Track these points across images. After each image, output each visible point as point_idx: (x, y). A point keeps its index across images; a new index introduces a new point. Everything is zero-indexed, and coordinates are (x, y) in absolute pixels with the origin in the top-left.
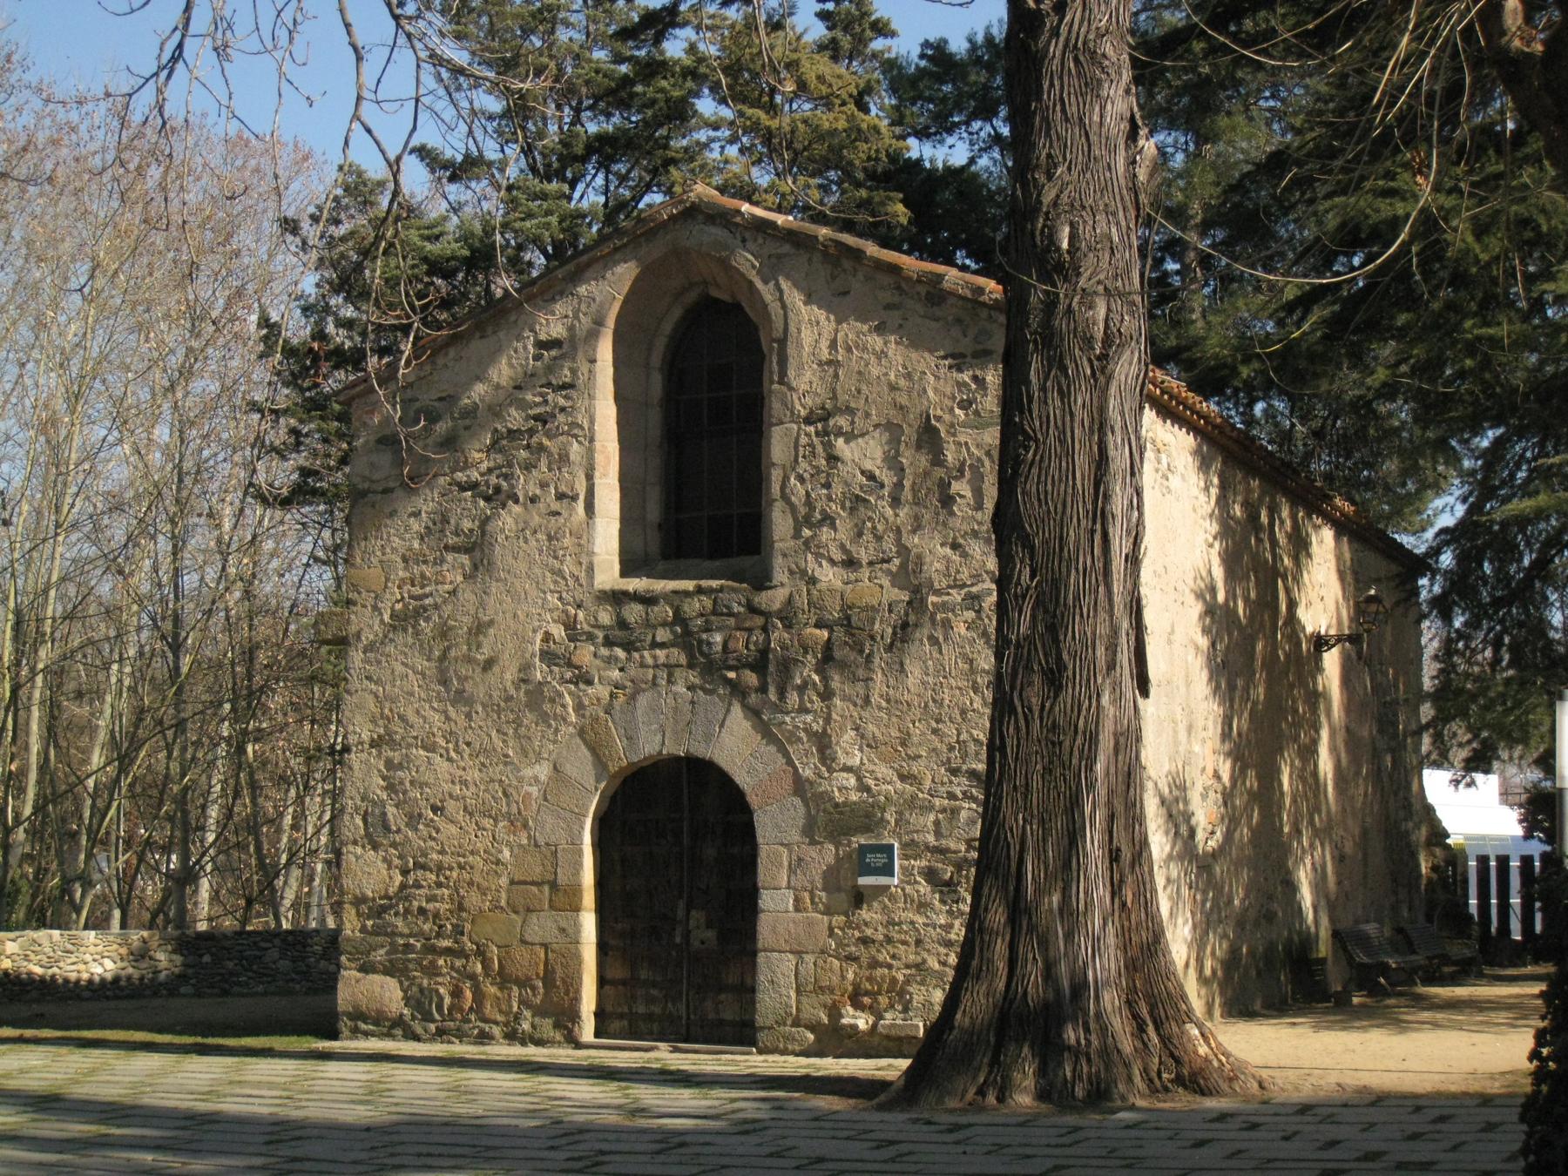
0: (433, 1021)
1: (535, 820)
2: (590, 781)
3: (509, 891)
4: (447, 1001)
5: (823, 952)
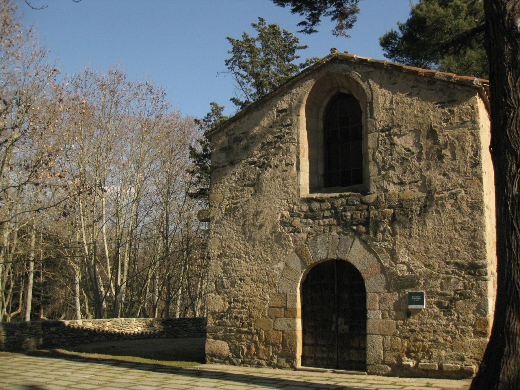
0: (240, 358)
1: (279, 284)
2: (299, 269)
3: (268, 310)
4: (245, 351)
5: (394, 335)
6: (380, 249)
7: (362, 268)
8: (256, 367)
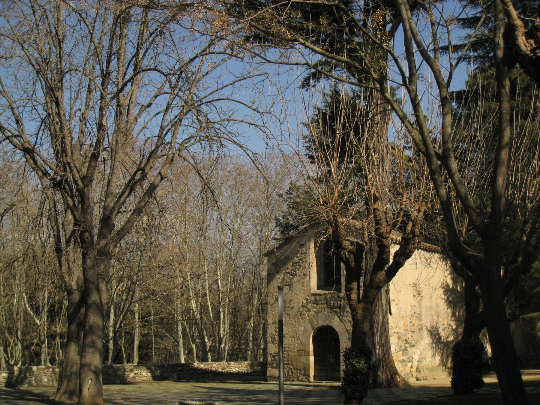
2: (311, 330)
4: (287, 374)
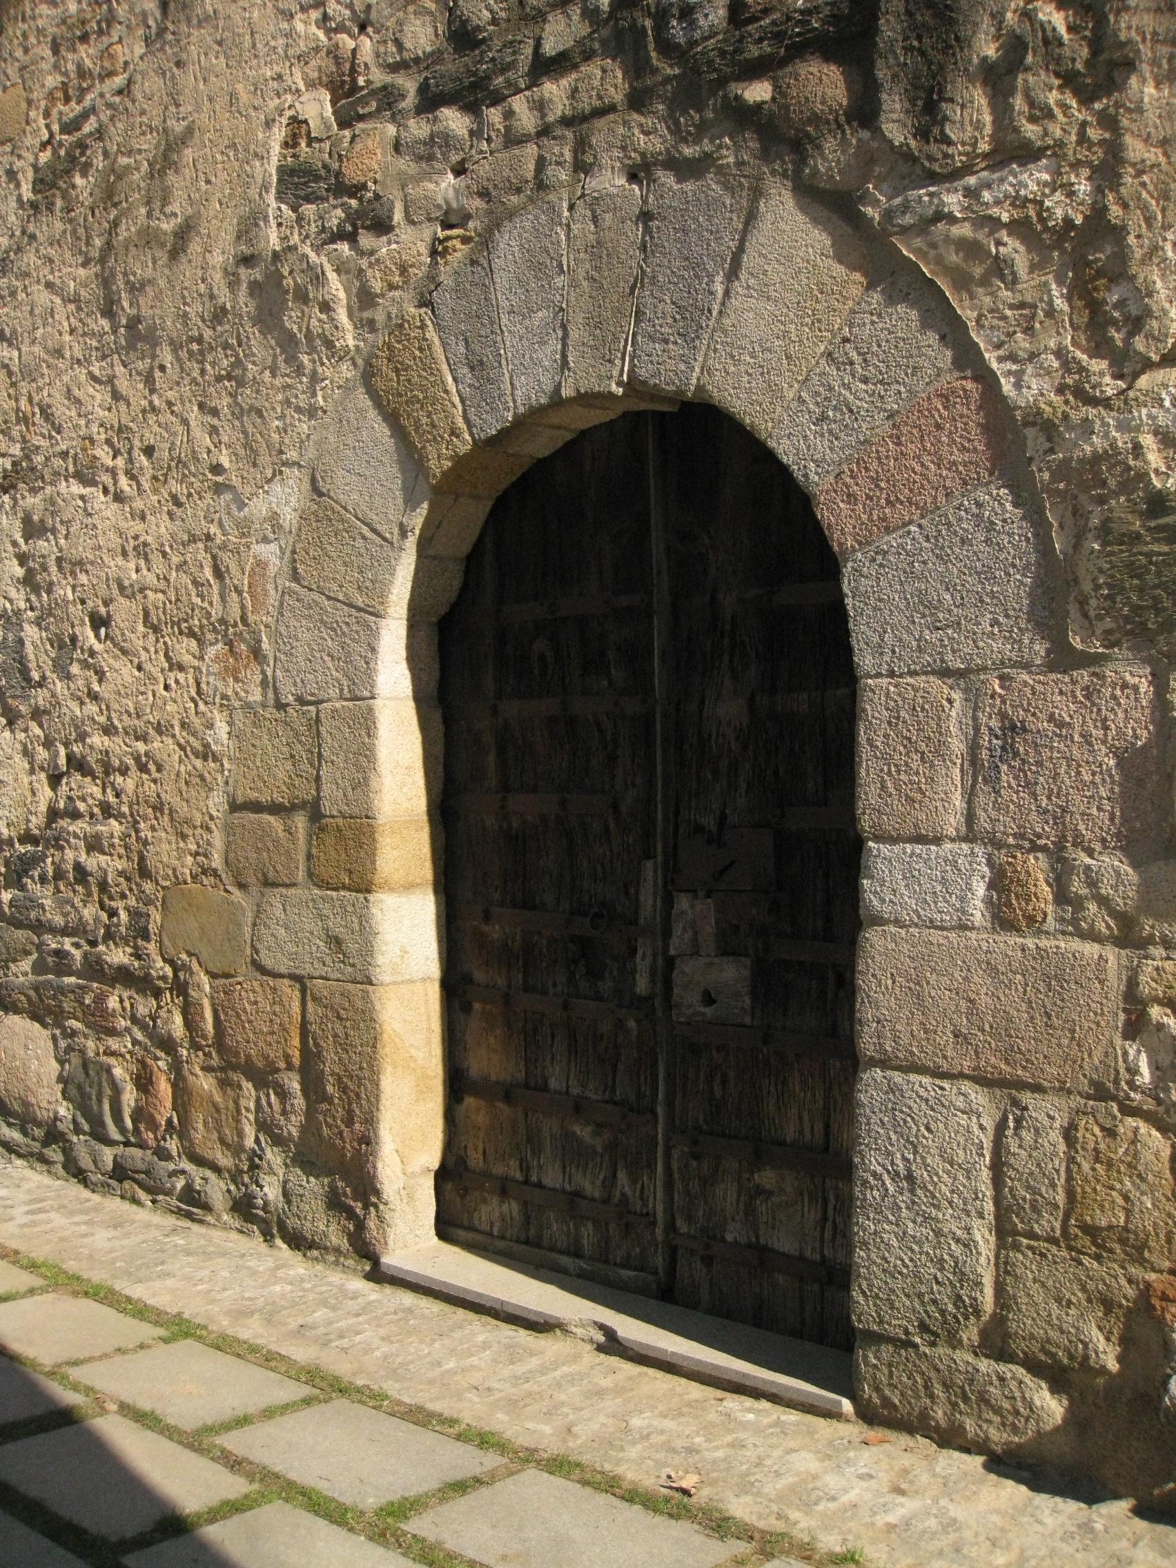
0: (110, 1143)
1: (276, 636)
3: (228, 829)
4: (129, 1097)
5: (1100, 1093)
6: (972, 249)
7: (821, 445)
8: (179, 1212)
